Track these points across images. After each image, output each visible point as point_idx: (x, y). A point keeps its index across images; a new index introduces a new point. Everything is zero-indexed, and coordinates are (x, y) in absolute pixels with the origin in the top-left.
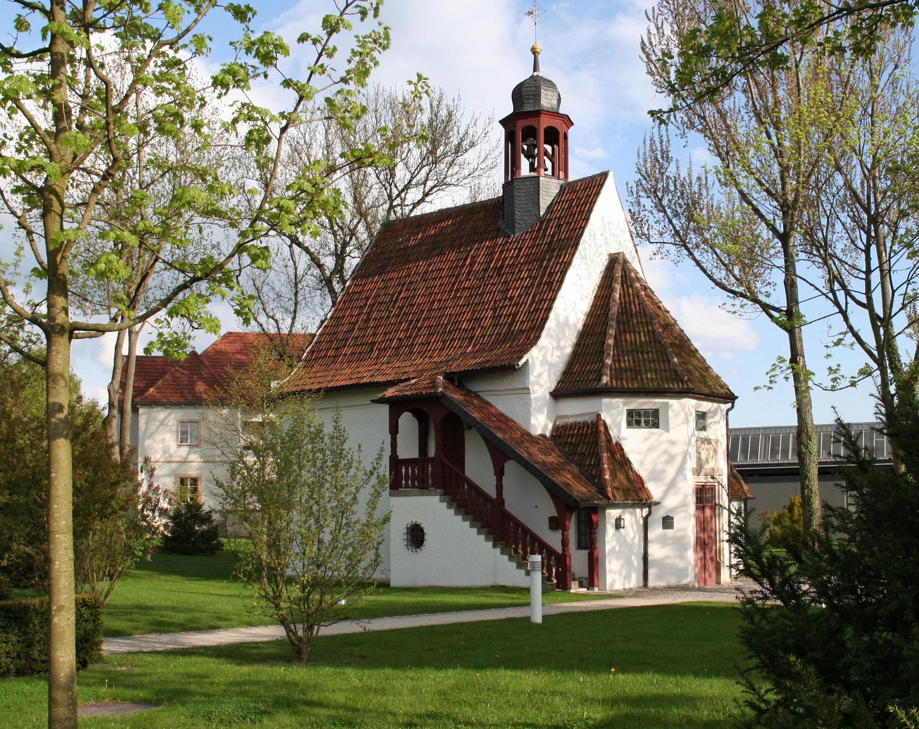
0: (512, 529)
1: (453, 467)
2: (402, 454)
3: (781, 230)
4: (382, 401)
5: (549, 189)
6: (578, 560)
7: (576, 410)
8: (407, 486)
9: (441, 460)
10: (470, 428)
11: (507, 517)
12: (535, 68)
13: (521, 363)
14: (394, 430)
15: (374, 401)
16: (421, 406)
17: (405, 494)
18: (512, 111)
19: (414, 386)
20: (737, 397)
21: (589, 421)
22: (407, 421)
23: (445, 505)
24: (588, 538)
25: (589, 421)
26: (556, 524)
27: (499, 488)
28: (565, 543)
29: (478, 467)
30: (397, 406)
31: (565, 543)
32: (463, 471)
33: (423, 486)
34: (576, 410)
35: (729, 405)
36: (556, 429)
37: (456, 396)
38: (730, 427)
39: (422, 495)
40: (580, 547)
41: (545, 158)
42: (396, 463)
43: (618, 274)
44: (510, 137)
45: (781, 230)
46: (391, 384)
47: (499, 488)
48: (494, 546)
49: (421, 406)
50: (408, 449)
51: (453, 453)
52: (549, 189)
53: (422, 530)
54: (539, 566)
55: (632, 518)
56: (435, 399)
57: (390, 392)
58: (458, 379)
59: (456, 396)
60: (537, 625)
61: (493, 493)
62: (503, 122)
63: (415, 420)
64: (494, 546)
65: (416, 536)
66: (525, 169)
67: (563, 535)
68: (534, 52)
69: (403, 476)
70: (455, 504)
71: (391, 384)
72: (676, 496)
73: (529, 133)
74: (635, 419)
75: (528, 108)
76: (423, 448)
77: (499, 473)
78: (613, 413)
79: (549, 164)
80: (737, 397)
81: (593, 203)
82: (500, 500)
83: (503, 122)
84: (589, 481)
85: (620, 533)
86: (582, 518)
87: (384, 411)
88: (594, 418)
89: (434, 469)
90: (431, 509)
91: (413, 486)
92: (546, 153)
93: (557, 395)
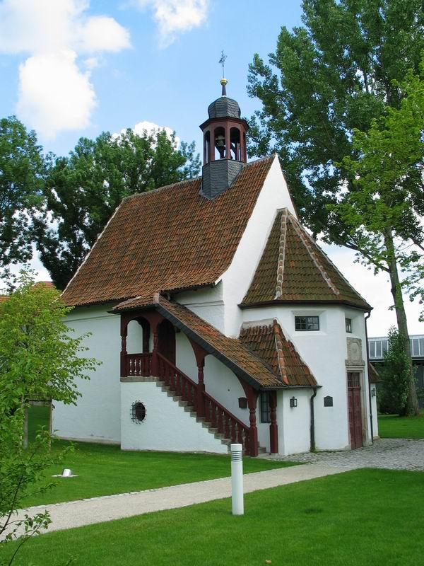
0: (211, 407)
1: (166, 360)
2: (130, 351)
3: (388, 267)
4: (115, 312)
5: (234, 168)
6: (263, 430)
7: (260, 318)
8: (133, 375)
9: (157, 355)
10: (179, 331)
11: (207, 398)
12: (224, 93)
13: (216, 282)
14: (124, 333)
15: (109, 312)
16: (144, 315)
17: (132, 381)
18: (208, 118)
19: (139, 299)
20: (373, 308)
21: (268, 326)
22: (134, 327)
23: (160, 389)
24: (269, 414)
25: (268, 326)
26: (242, 403)
27: (201, 376)
28: (252, 420)
29: (185, 360)
30: (126, 315)
31: (252, 420)
32: (175, 365)
33: (146, 373)
34: (260, 318)
35: (366, 314)
36: (243, 331)
37: (169, 307)
38: (368, 337)
39: (144, 381)
40: (263, 421)
41: (231, 150)
42: (125, 357)
43: (284, 229)
44: (207, 137)
45: (388, 267)
46: (123, 300)
47: (201, 376)
48: (198, 421)
49: (144, 315)
50: (135, 347)
51: (167, 349)
52: (234, 168)
53: (143, 408)
54: (240, 455)
55: (303, 400)
56: (153, 309)
57: (124, 305)
58: (172, 296)
59: (169, 307)
60: (242, 516)
61: (196, 380)
62: (202, 127)
63: (140, 326)
64: (198, 421)
65: (139, 411)
66: (217, 156)
67: (251, 413)
68: (223, 84)
69: (130, 367)
70: (168, 388)
71: (123, 300)
72: (332, 381)
73: (220, 132)
74: (301, 324)
75: (220, 115)
76: (146, 346)
77: (201, 364)
78: (285, 318)
79: (233, 155)
80: (373, 308)
81: (265, 174)
82: (202, 385)
83: (202, 127)
84: (270, 376)
85: (293, 421)
86: (264, 398)
87: (116, 321)
88: (271, 323)
89: (152, 363)
90: (150, 391)
91: (138, 375)
92: (232, 147)
93: (243, 307)
